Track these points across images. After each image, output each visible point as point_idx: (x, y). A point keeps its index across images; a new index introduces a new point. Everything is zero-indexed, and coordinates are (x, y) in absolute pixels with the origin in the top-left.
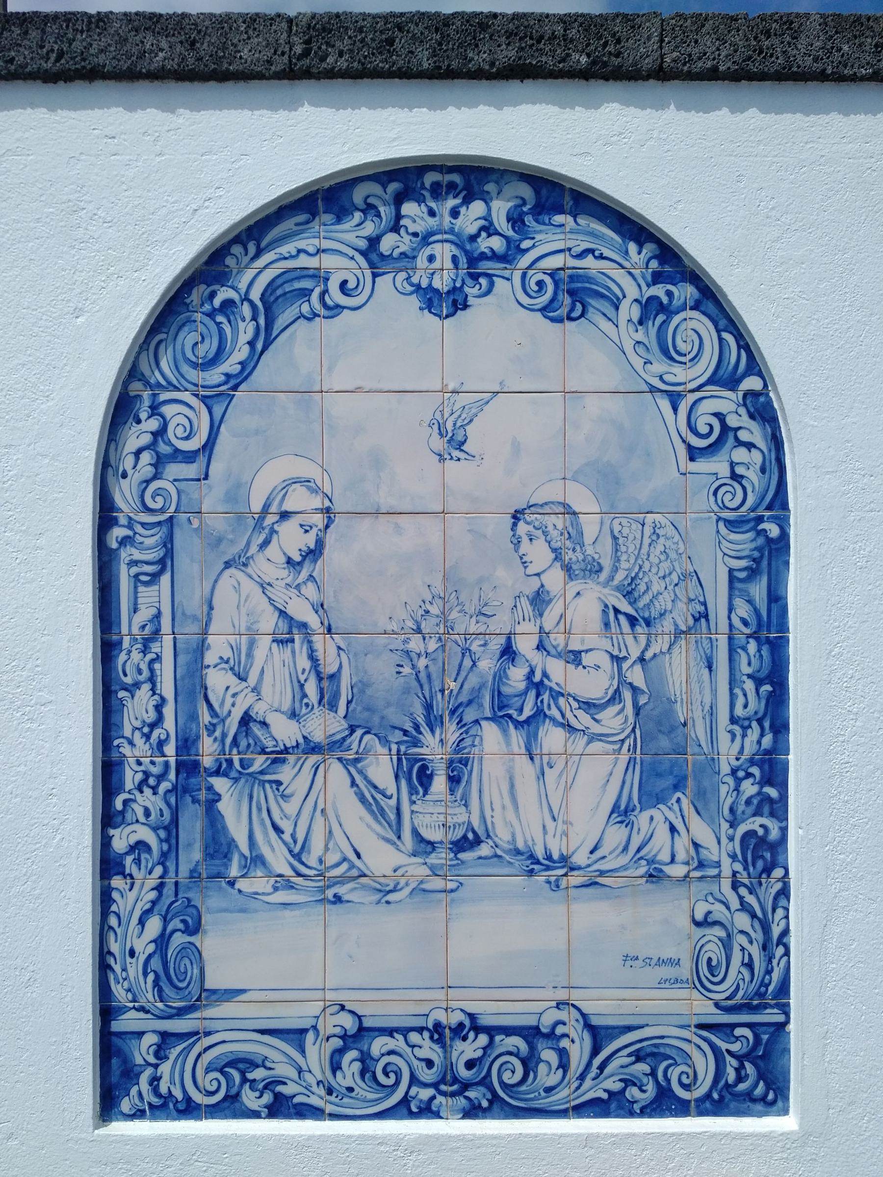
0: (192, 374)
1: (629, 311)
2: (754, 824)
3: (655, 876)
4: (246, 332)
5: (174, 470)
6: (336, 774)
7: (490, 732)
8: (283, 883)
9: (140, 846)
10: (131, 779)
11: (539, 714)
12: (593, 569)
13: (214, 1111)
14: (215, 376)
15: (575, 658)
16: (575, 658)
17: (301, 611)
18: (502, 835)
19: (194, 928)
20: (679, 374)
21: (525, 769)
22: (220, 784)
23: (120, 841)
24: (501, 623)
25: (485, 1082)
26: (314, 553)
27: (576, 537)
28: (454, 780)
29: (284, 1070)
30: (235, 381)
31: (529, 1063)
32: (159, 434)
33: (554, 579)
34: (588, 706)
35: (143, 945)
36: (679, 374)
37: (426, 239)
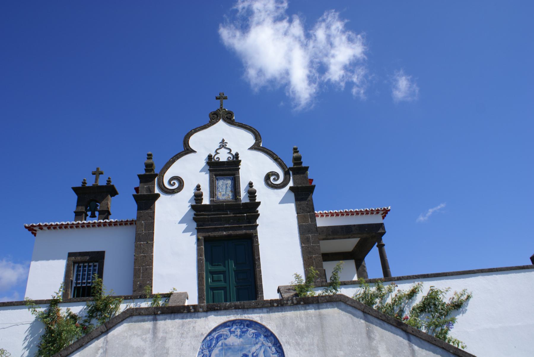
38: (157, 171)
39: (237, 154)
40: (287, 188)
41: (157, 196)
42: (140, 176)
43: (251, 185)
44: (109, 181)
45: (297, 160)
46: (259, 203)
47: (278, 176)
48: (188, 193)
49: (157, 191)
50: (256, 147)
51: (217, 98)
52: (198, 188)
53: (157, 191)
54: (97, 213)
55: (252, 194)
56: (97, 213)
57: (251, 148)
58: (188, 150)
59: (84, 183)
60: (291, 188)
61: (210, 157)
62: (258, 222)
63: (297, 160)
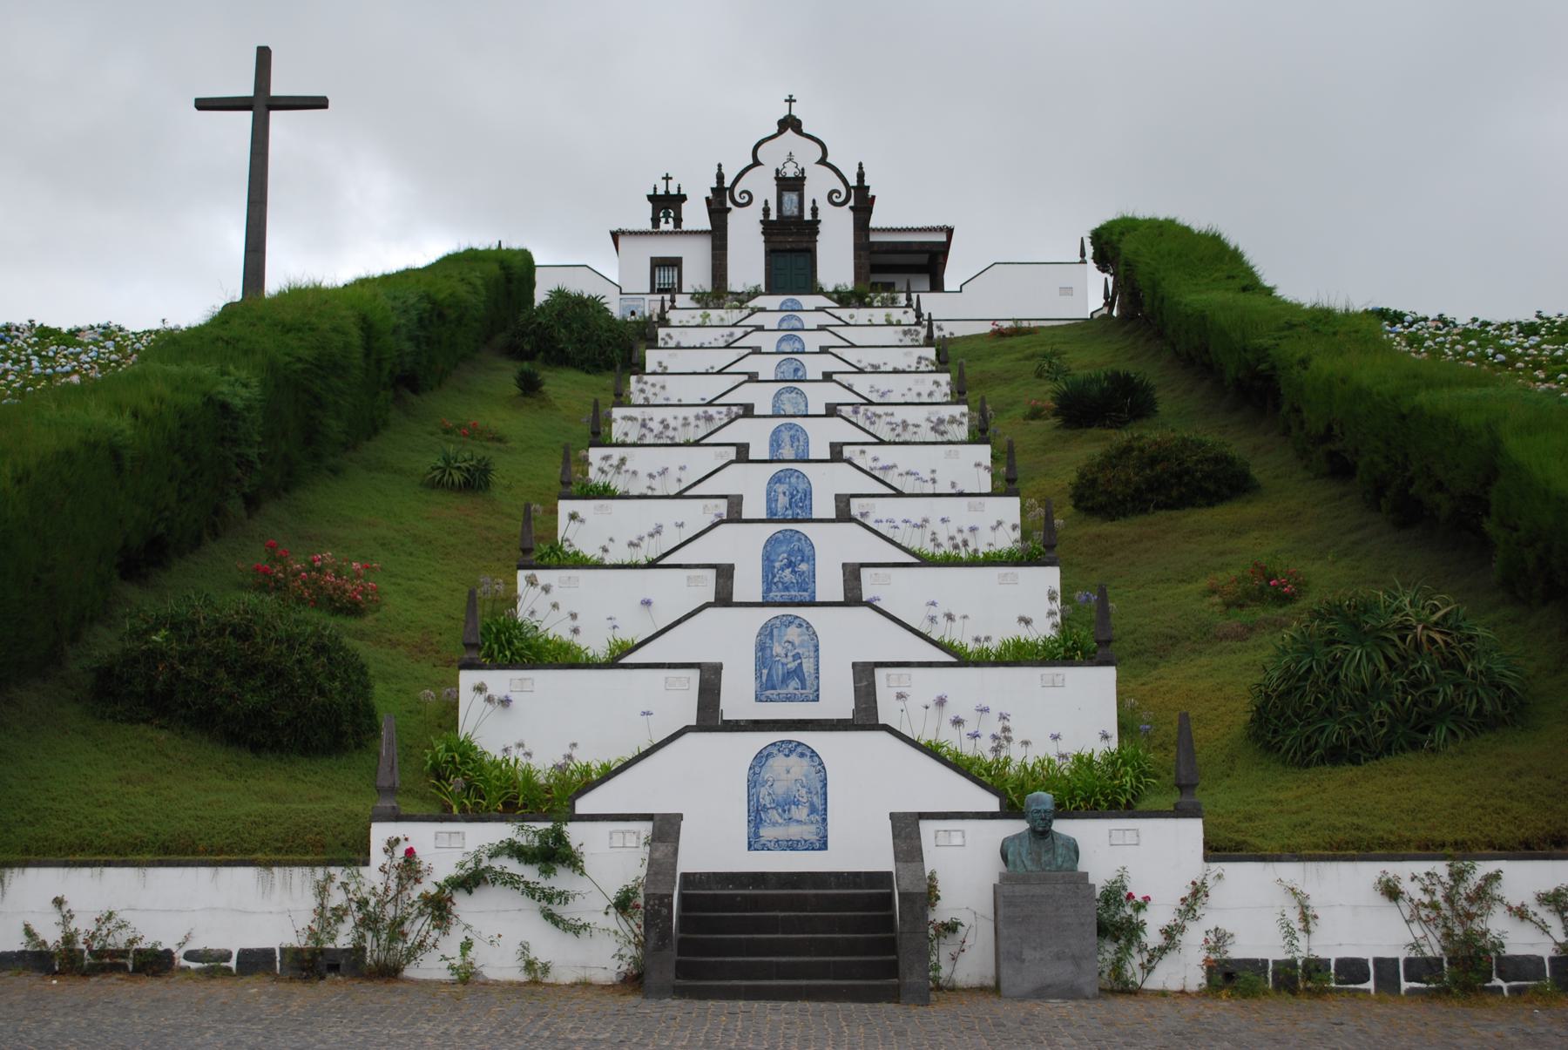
38: (727, 184)
39: (803, 169)
41: (730, 209)
43: (814, 201)
44: (679, 188)
45: (861, 176)
48: (758, 206)
49: (729, 204)
50: (823, 161)
51: (786, 101)
52: (766, 202)
54: (671, 220)
55: (815, 211)
56: (671, 220)
57: (817, 163)
58: (756, 163)
59: (655, 189)
60: (851, 208)
61: (777, 170)
62: (818, 237)
63: (861, 176)
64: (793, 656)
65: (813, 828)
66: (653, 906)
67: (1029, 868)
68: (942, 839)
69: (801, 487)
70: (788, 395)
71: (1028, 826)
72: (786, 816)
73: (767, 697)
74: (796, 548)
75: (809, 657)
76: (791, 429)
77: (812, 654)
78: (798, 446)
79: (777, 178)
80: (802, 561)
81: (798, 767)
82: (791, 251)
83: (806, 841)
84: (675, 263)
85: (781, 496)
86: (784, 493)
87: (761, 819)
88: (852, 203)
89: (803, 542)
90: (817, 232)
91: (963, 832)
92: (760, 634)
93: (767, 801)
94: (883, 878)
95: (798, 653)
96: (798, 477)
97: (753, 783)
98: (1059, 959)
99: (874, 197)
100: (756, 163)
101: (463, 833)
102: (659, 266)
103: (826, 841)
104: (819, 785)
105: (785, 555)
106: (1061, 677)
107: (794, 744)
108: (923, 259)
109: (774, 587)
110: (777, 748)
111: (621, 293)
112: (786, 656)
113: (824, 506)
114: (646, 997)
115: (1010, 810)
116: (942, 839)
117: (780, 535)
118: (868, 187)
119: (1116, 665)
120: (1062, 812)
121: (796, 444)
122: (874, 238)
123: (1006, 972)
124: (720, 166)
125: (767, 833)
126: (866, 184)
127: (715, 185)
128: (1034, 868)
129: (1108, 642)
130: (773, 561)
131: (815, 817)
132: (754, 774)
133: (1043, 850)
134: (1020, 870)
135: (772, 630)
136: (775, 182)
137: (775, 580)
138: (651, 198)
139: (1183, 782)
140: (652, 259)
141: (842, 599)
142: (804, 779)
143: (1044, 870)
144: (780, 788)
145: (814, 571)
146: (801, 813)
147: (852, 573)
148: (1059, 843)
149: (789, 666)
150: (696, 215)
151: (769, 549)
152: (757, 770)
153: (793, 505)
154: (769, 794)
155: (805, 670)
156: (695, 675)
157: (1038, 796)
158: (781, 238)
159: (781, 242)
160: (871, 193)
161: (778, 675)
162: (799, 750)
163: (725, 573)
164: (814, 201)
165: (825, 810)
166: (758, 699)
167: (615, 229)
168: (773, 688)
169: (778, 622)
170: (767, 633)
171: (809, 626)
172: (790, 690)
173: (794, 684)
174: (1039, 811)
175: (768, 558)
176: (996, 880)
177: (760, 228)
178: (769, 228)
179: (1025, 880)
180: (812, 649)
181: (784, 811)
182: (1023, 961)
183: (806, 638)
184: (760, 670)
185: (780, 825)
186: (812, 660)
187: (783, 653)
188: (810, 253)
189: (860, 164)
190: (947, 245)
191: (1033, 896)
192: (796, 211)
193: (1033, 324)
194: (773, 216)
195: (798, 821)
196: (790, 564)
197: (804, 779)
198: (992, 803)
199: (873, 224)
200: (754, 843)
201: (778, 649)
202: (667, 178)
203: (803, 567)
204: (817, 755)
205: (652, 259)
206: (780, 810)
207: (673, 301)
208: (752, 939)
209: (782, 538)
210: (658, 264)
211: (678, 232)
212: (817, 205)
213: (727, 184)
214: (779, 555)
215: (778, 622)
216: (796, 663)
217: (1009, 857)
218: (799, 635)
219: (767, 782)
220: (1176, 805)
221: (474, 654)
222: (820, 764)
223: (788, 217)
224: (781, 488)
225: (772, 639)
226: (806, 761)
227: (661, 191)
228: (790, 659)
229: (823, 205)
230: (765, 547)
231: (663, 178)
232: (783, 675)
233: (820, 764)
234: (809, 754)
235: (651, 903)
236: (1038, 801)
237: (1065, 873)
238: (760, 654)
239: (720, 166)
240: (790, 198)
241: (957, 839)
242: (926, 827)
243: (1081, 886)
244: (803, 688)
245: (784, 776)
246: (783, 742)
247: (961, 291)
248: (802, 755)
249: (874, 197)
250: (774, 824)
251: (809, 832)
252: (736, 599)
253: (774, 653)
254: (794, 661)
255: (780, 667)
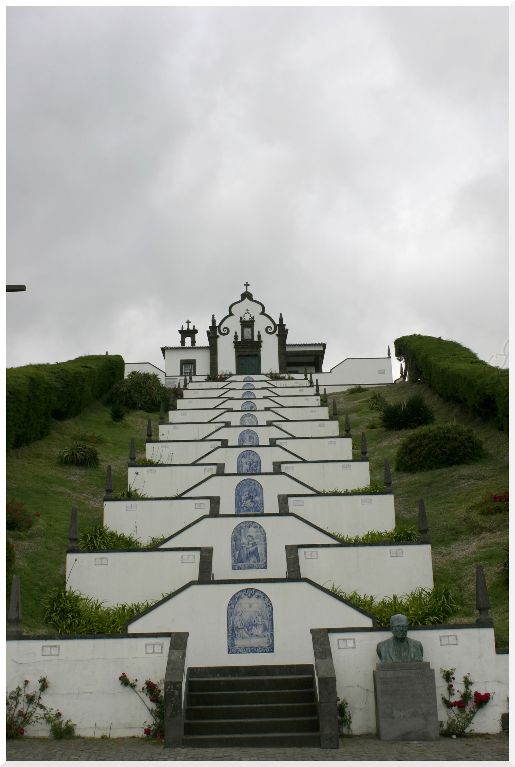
0: (233, 603)
1: (262, 598)
2: (271, 632)
3: (265, 636)
4: (237, 600)
5: (232, 609)
6: (243, 630)
7: (253, 627)
8: (240, 638)
9: (230, 635)
10: (229, 630)
11: (257, 625)
12: (260, 615)
13: (235, 653)
14: (235, 603)
15: (259, 621)
16: (259, 621)
17: (240, 619)
18: (254, 634)
19: (234, 640)
20: (265, 602)
21: (256, 630)
22: (235, 631)
23: (229, 635)
24: (254, 619)
25: (253, 651)
26: (241, 615)
27: (259, 613)
28: (251, 630)
29: (240, 650)
30: (236, 603)
31: (257, 649)
32: (231, 607)
33: (258, 616)
34: (260, 625)
35: (231, 642)
36: (265, 602)
37: (248, 593)
38: (217, 324)
39: (253, 317)
40: (275, 334)
41: (218, 336)
42: (210, 327)
43: (259, 332)
44: (194, 327)
45: (281, 320)
46: (262, 341)
47: (271, 329)
49: (218, 334)
50: (263, 313)
51: (245, 285)
52: (236, 333)
53: (218, 334)
55: (259, 336)
58: (231, 314)
59: (182, 327)
60: (277, 335)
61: (241, 318)
63: (281, 320)
64: (253, 544)
65: (265, 640)
66: (170, 690)
67: (395, 660)
68: (342, 644)
69: (255, 460)
70: (248, 418)
71: (392, 635)
72: (250, 633)
73: (239, 567)
74: (253, 488)
75: (261, 544)
76: (249, 433)
77: (263, 542)
78: (253, 441)
79: (241, 321)
80: (256, 495)
81: (256, 604)
82: (248, 356)
83: (261, 647)
84: (192, 363)
85: (245, 465)
86: (246, 463)
87: (235, 635)
88: (277, 332)
89: (257, 485)
90: (260, 347)
91: (354, 640)
92: (234, 532)
93: (238, 624)
94: (307, 669)
95: (255, 542)
96: (253, 455)
97: (230, 614)
98: (415, 716)
99: (287, 330)
100: (231, 314)
101: (59, 647)
102: (185, 364)
103: (273, 647)
104: (268, 614)
105: (247, 493)
106: (401, 551)
107: (253, 591)
108: (312, 359)
109: (242, 510)
110: (244, 593)
111: (166, 376)
112: (249, 543)
113: (267, 467)
114: (166, 747)
115: (377, 627)
116: (445, 641)
117: (244, 482)
118: (285, 325)
119: (431, 544)
120: (414, 626)
121: (252, 440)
122: (288, 349)
123: (383, 725)
124: (213, 316)
125: (239, 643)
126: (284, 323)
127: (211, 325)
128: (397, 660)
129: (426, 531)
130: (241, 496)
131: (267, 633)
132: (231, 608)
133: (402, 649)
134: (389, 661)
135: (240, 529)
136: (240, 323)
137: (242, 506)
138: (181, 332)
139: (482, 606)
140: (181, 360)
141: (277, 511)
142: (259, 611)
143: (403, 661)
144: (246, 617)
145: (263, 501)
146: (258, 631)
147: (283, 500)
148: (411, 645)
149: (250, 549)
150: (202, 340)
151: (238, 489)
152: (233, 606)
153: (251, 469)
154: (240, 620)
155: (259, 552)
156: (197, 555)
157: (398, 617)
158: (243, 350)
159: (243, 351)
160: (286, 328)
161: (244, 554)
162: (257, 594)
163: (215, 501)
164: (259, 332)
165: (272, 629)
166: (233, 568)
167: (163, 346)
168: (242, 562)
169: (244, 525)
170: (238, 531)
171: (261, 527)
172: (251, 562)
173: (253, 559)
174: (399, 626)
175: (238, 494)
176: (374, 668)
177: (233, 345)
178: (237, 345)
179: (393, 668)
180: (263, 539)
181: (249, 630)
182: (393, 718)
183: (259, 533)
184: (234, 552)
185: (247, 638)
186: (262, 546)
187: (247, 542)
188: (257, 356)
189: (281, 315)
190: (323, 352)
191: (398, 677)
192: (250, 337)
193: (367, 386)
194: (239, 339)
195: (256, 636)
196: (250, 497)
197: (259, 611)
198: (368, 623)
199: (288, 342)
200: (231, 649)
201: (244, 540)
202: (188, 322)
203: (257, 499)
204: (267, 597)
205: (181, 360)
206: (246, 630)
207: (191, 378)
208: (231, 708)
209: (245, 483)
210: (185, 363)
211: (194, 347)
212: (261, 334)
213: (217, 324)
214: (244, 492)
215: (244, 525)
216: (254, 547)
217: (382, 654)
218: (255, 532)
219: (238, 613)
220: (477, 621)
221: (74, 544)
222: (269, 602)
223: (247, 340)
224: (245, 460)
225: (240, 534)
226: (260, 601)
227: (185, 328)
228: (251, 545)
229: (264, 334)
230: (236, 488)
231: (186, 322)
232: (247, 554)
233: (269, 602)
234: (262, 596)
235: (169, 687)
236: (398, 619)
237: (416, 663)
238: (234, 543)
239: (213, 316)
240: (248, 331)
241: (350, 644)
242: (333, 638)
243: (426, 671)
244: (258, 561)
245: (248, 609)
246: (247, 589)
247: (331, 372)
248: (258, 597)
249: (287, 330)
250: (243, 638)
251: (263, 642)
252: (221, 513)
253: (242, 543)
254: (253, 546)
255: (245, 550)
